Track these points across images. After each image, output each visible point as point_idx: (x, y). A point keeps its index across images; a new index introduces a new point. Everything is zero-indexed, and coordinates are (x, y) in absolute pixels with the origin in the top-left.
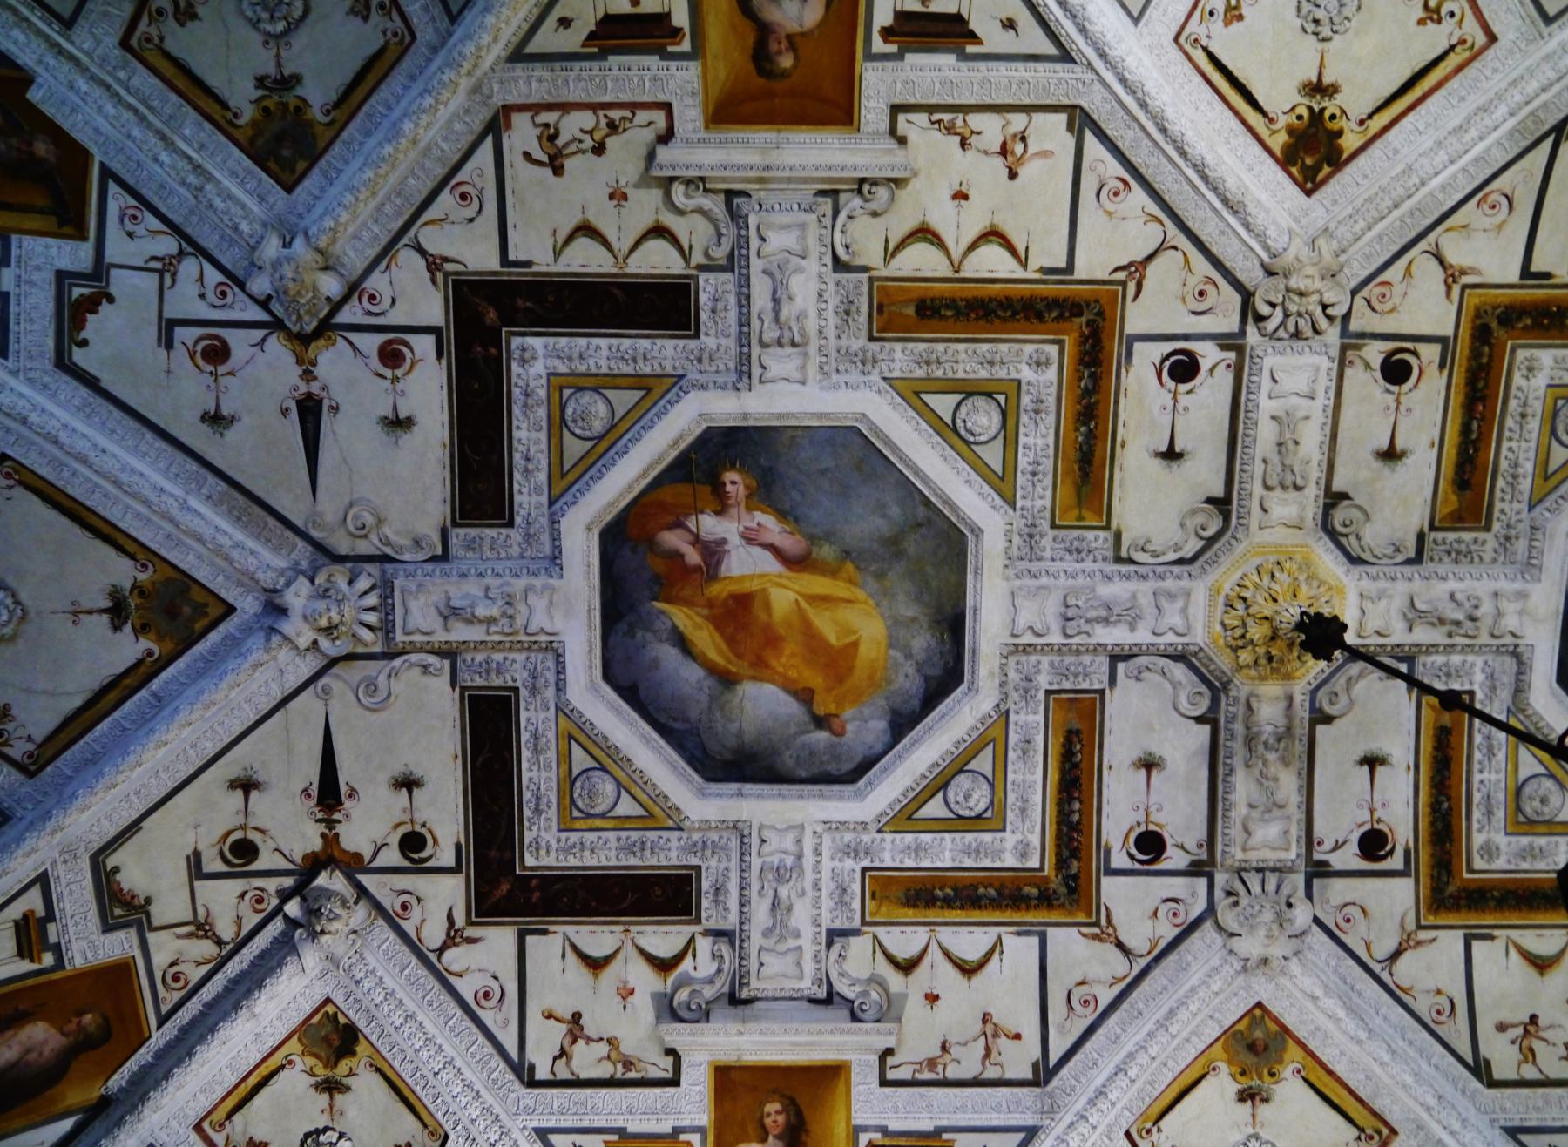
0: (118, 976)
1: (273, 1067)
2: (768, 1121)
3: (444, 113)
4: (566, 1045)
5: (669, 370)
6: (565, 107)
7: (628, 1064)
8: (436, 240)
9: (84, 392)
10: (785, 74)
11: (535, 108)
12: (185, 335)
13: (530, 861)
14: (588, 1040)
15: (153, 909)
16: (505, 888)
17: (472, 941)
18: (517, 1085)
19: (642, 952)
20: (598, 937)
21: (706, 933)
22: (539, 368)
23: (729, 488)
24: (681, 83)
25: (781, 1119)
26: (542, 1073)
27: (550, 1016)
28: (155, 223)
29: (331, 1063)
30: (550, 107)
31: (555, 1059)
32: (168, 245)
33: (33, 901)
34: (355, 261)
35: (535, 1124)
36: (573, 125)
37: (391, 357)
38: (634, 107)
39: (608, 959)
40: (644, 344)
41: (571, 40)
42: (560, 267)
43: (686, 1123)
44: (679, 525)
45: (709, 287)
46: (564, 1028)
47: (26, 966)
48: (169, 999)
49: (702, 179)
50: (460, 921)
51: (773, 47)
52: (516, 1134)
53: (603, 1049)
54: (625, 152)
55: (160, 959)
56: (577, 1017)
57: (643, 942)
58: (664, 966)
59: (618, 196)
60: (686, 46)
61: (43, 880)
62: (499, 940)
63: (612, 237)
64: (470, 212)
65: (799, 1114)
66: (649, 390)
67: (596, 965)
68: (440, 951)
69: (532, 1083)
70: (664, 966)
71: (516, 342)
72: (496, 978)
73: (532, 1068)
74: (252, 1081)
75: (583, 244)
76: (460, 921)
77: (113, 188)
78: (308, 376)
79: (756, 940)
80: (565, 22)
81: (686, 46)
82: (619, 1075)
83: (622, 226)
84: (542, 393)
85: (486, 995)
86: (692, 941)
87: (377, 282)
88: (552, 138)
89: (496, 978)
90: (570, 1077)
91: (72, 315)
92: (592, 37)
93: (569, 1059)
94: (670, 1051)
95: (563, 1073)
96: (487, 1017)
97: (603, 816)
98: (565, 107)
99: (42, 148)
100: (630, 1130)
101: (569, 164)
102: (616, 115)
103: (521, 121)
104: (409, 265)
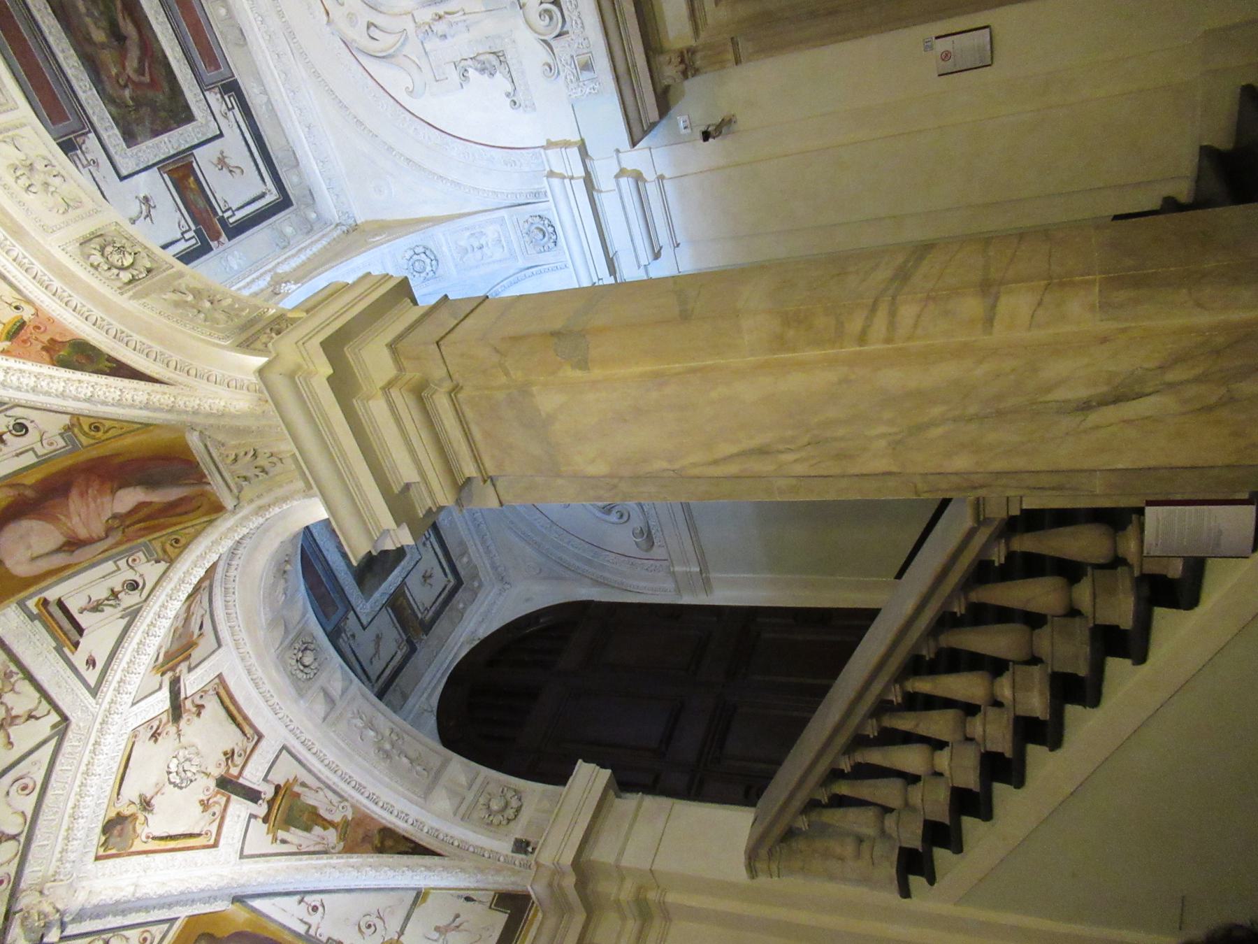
1: (157, 842)
4: (22, 720)
14: (8, 710)
18: (73, 727)
26: (55, 718)
27: (11, 743)
29: (133, 817)
31: (37, 719)
35: (91, 699)
43: (23, 617)
48: (157, 931)
52: (105, 705)
68: (14, 837)
69: (65, 718)
72: (8, 793)
73: (54, 727)
74: (172, 844)
82: (21, 675)
85: (24, 788)
89: (8, 793)
90: (44, 702)
93: (31, 711)
95: (45, 706)
96: (39, 777)
100: (54, 644)
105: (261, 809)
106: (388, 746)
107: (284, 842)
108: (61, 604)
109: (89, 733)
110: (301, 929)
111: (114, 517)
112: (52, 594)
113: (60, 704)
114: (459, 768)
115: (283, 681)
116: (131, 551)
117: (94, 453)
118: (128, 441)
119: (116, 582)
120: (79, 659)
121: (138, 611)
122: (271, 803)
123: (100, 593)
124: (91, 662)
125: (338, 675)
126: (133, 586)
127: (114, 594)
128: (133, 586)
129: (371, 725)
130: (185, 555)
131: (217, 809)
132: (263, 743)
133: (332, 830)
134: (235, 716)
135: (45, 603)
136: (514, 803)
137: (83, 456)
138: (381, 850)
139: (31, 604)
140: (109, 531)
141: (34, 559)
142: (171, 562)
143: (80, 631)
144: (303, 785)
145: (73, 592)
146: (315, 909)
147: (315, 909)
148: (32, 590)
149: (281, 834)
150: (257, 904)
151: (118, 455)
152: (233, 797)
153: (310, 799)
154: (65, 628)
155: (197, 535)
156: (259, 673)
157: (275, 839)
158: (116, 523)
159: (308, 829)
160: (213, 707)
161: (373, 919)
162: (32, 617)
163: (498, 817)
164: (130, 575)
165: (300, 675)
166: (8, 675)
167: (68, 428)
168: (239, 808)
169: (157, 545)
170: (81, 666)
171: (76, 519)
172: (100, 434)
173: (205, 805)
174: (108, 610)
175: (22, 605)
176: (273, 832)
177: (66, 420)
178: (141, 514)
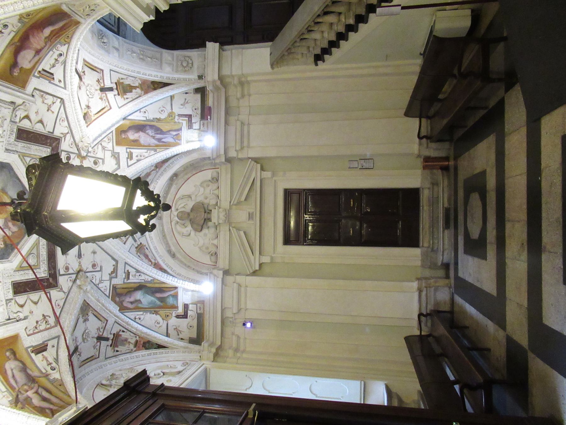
0: (118, 143)
2: (19, 71)
3: (67, 321)
5: (17, 272)
6: (46, 329)
7: (42, 96)
8: (62, 295)
9: (115, 257)
10: (7, 350)
11: (51, 328)
12: (98, 269)
13: (49, 150)
15: (111, 155)
16: (54, 145)
17: (62, 134)
18: (65, 100)
19: (31, 122)
20: (39, 128)
21: (16, 123)
22: (42, 269)
23: (2, 243)
24: (28, 342)
25: (15, 71)
26: (59, 100)
28: (102, 289)
29: (87, 112)
30: (49, 329)
32: (100, 286)
33: (130, 163)
34: (75, 288)
36: (43, 326)
37: (67, 268)
38: (34, 334)
39: (38, 122)
40: (22, 278)
41: (50, 344)
42: (40, 293)
44: (13, 233)
45: (10, 295)
46: (51, 109)
47: (132, 150)
48: (110, 136)
49: (18, 321)
50: (63, 139)
51: (12, 356)
52: (70, 90)
53: (45, 101)
54: (31, 323)
55: (111, 144)
56: (48, 111)
57: (30, 124)
58: (27, 117)
59: (31, 312)
60: (29, 350)
61: (128, 166)
62: (57, 133)
63: (30, 302)
64: (57, 302)
65: (10, 70)
66: (20, 267)
67: (41, 122)
68: (68, 133)
69: (62, 99)
70: (27, 117)
71: (46, 275)
74: (100, 113)
75: (36, 300)
76: (63, 139)
77: (108, 295)
78: (80, 263)
79: (8, 120)
80: (53, 346)
81: (29, 350)
83: (29, 306)
84: (41, 263)
86: (20, 121)
87: (70, 284)
88: (46, 322)
91: (115, 271)
92: (47, 345)
94: (33, 96)
95: (55, 98)
97: (33, 158)
98: (46, 329)
99: (117, 299)
101: (41, 317)
102: (36, 331)
103: (53, 324)
104: (66, 289)
105: (116, 92)
106: (142, 57)
107: (127, 98)
108: (44, 70)
109: (70, 99)
110: (145, 119)
111: (46, 38)
112: (40, 69)
113: (59, 96)
114: (167, 54)
115: (102, 52)
116: (55, 46)
117: (31, 23)
118: (40, 14)
119: (55, 56)
120: (56, 82)
121: (65, 61)
122: (117, 89)
123: (53, 61)
124: (60, 81)
125: (115, 39)
126: (61, 55)
127: (56, 60)
128: (61, 55)
129: (133, 52)
130: (72, 40)
131: (105, 98)
132: (105, 72)
133: (138, 89)
134: (93, 68)
135: (40, 72)
136: (190, 62)
137: (28, 25)
138: (155, 89)
139: (36, 74)
140: (46, 43)
141: (30, 62)
142: (69, 43)
143: (52, 74)
144: (122, 79)
145: (45, 65)
146: (145, 112)
147: (145, 112)
148: (34, 70)
149: (125, 97)
150: (129, 118)
151: (38, 21)
152: (107, 92)
153: (127, 82)
154: (48, 75)
155: (74, 33)
156: (93, 52)
157: (124, 99)
158: (47, 40)
159: (131, 92)
160: (87, 70)
161: (162, 109)
162: (38, 78)
163: (187, 67)
164: (58, 53)
165: (105, 47)
166: (42, 96)
167: (20, 19)
168: (110, 95)
169: (62, 41)
170: (58, 84)
171: (35, 44)
172: (30, 16)
173: (101, 99)
174: (57, 65)
175: (34, 76)
176: (122, 97)
177: (18, 17)
178: (54, 34)
